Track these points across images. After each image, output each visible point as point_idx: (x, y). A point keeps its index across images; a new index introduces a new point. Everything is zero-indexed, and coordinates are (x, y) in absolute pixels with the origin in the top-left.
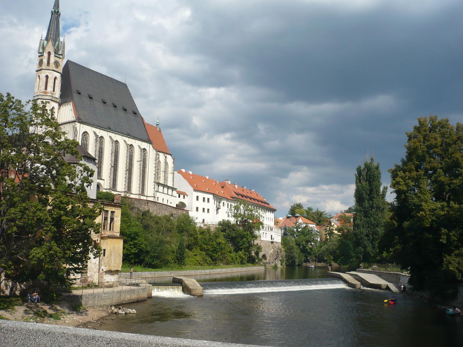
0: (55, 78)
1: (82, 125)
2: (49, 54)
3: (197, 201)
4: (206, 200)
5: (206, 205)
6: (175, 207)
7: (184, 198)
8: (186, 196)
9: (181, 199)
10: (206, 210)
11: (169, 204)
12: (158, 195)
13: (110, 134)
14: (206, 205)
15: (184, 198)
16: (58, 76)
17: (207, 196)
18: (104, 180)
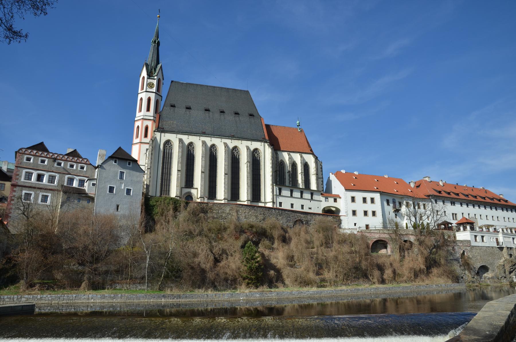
0: (149, 100)
1: (163, 134)
2: (144, 78)
3: (353, 204)
4: (369, 200)
5: (369, 207)
6: (320, 212)
7: (335, 200)
8: (338, 199)
9: (330, 203)
10: (370, 213)
11: (306, 210)
12: (280, 199)
13: (203, 139)
14: (369, 207)
15: (335, 200)
16: (153, 96)
17: (369, 196)
18: (197, 189)
